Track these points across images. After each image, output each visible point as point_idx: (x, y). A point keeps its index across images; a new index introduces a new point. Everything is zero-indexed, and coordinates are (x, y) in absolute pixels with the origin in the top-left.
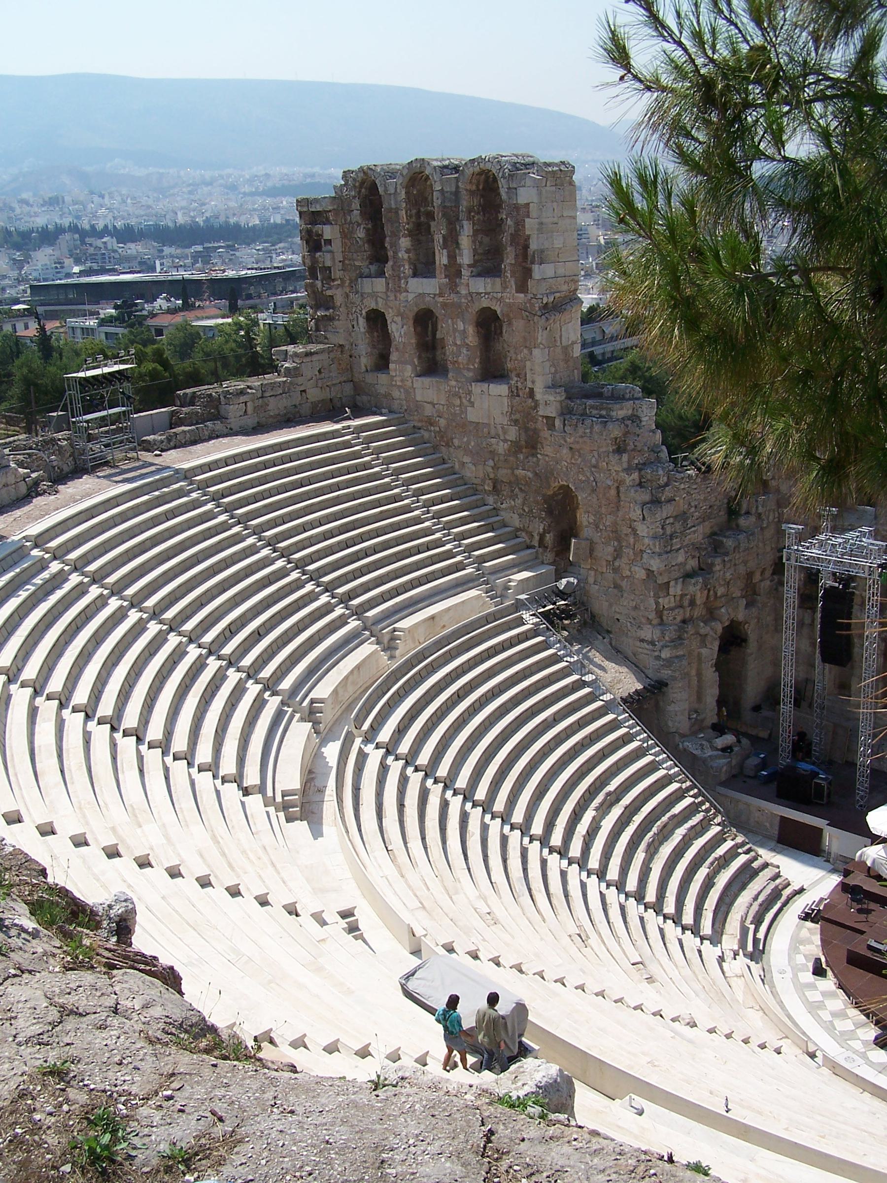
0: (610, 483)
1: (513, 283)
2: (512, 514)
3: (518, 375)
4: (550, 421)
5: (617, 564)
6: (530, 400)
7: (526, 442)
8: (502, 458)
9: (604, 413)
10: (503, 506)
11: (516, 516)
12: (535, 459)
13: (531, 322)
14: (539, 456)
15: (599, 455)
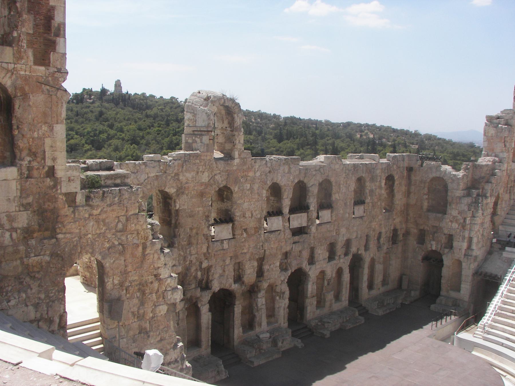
0: (135, 241)
1: (30, 53)
2: (25, 309)
3: (33, 154)
4: (71, 198)
5: (141, 311)
6: (48, 180)
7: (40, 225)
8: (11, 249)
9: (118, 181)
10: (13, 303)
11: (31, 308)
12: (54, 240)
13: (54, 97)
14: (60, 236)
15: (127, 220)
